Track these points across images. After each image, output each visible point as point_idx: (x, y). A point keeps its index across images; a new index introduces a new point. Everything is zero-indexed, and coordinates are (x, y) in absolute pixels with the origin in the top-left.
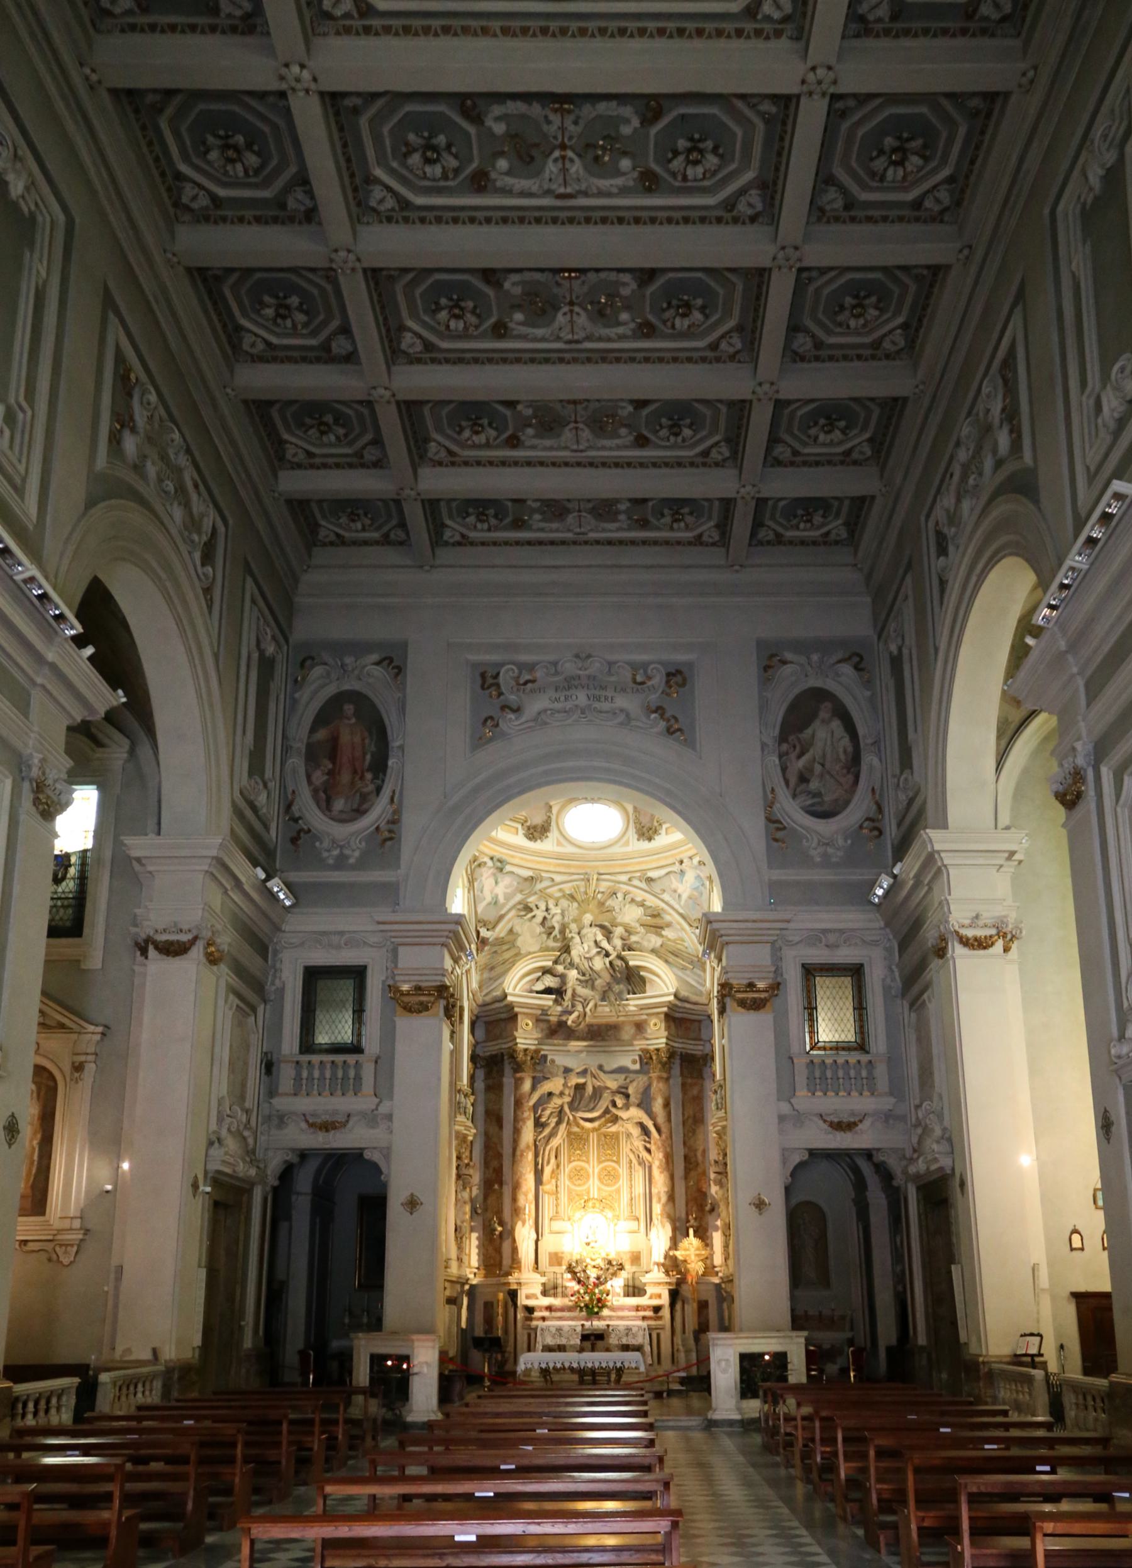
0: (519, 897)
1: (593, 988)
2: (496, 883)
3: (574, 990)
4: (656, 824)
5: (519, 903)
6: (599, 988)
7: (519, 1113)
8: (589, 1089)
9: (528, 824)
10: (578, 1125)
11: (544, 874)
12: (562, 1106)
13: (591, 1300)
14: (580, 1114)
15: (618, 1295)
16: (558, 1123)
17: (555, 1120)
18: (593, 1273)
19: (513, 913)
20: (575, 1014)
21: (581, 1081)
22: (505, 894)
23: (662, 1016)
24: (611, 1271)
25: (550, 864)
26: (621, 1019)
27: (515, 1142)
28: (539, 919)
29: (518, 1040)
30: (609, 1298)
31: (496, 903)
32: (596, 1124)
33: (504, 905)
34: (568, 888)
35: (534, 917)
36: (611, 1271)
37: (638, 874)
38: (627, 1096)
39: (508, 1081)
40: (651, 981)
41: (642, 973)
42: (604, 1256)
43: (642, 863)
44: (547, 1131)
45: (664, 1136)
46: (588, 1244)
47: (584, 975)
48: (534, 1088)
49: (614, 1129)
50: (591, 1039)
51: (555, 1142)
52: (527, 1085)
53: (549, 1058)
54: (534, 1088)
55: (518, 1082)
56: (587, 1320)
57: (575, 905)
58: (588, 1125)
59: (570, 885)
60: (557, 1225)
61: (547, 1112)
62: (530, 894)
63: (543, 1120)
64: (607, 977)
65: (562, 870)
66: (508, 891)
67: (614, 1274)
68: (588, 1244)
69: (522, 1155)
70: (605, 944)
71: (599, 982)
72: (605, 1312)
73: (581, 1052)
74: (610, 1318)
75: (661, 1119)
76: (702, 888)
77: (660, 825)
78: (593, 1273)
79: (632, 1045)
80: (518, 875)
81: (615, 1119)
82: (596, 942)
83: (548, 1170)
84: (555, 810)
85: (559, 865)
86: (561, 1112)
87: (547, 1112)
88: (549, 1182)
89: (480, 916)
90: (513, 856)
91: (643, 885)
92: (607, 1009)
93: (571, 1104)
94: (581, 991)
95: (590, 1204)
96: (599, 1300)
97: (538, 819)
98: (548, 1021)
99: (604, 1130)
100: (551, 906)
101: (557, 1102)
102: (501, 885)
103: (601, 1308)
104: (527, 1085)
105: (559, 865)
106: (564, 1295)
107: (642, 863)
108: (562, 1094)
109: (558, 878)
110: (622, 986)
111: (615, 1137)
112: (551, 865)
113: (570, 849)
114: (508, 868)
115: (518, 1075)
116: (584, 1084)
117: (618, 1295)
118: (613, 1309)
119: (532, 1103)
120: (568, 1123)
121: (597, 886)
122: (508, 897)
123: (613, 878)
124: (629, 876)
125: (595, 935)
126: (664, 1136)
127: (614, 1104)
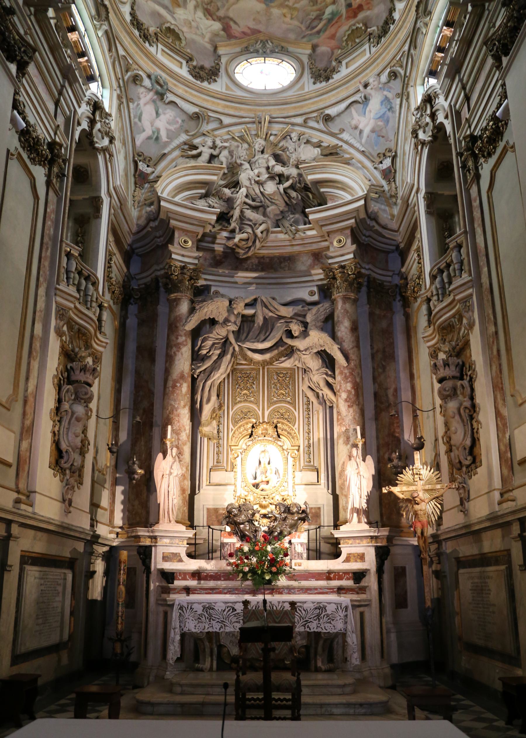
0: (184, 137)
1: (265, 215)
2: (157, 114)
3: (242, 212)
4: (334, 63)
5: (185, 143)
6: (272, 216)
7: (173, 338)
8: (260, 320)
9: (195, 63)
10: (245, 357)
11: (211, 114)
12: (227, 339)
13: (260, 562)
14: (248, 345)
15: (300, 556)
16: (221, 356)
17: (218, 352)
18: (263, 525)
19: (177, 153)
20: (245, 236)
21: (250, 312)
22: (168, 130)
23: (348, 232)
24: (290, 521)
25: (218, 104)
26: (297, 249)
27: (167, 372)
28: (205, 156)
29: (173, 256)
30: (287, 560)
31: (157, 139)
32: (267, 356)
33: (166, 144)
34: (237, 130)
35: (199, 155)
36: (290, 521)
37: (315, 114)
38: (305, 325)
39: (162, 309)
40: (334, 197)
41: (322, 190)
42: (278, 499)
43: (321, 100)
44: (208, 364)
45: (352, 364)
46: (256, 486)
47: (254, 200)
48: (192, 310)
49: (288, 364)
50: (262, 270)
51: (219, 376)
52: (184, 307)
53: (213, 289)
54: (192, 310)
55: (174, 304)
56: (254, 592)
57: (246, 146)
58: (258, 357)
59: (239, 127)
60: (218, 476)
61: (209, 343)
62: (194, 136)
63: (204, 352)
64: (282, 206)
65: (232, 112)
66: (172, 128)
67: (294, 526)
68: (256, 486)
69: (174, 386)
70: (279, 169)
71: (271, 209)
72: (282, 581)
73: (250, 284)
74: (290, 590)
75: (348, 344)
76: (390, 114)
77: (340, 62)
78: (263, 525)
79: (311, 275)
80: (182, 110)
81: (291, 352)
82: (268, 168)
83: (207, 409)
84: (224, 60)
85: (227, 107)
86: (226, 342)
87: (209, 343)
88: (209, 424)
89: (138, 149)
90: (175, 85)
91: (321, 126)
92: (282, 236)
93: (238, 334)
94: (249, 214)
95: (259, 430)
96: (273, 562)
97: (208, 64)
98: (213, 250)
99: (277, 365)
100: (218, 143)
101: (220, 332)
102: (162, 117)
103: (276, 575)
104: (184, 307)
105: (227, 107)
106: (222, 557)
107: (321, 100)
108: (226, 321)
109: (226, 120)
110: (297, 216)
111: (291, 373)
112: (219, 106)
113: (239, 93)
114: (170, 97)
115: (173, 296)
116: (254, 316)
117: (300, 556)
118: (292, 577)
119: (191, 325)
120: (233, 355)
121: (269, 128)
122: (171, 136)
123: (287, 120)
124: (304, 117)
125: (268, 161)
126: (352, 364)
127: (289, 334)
